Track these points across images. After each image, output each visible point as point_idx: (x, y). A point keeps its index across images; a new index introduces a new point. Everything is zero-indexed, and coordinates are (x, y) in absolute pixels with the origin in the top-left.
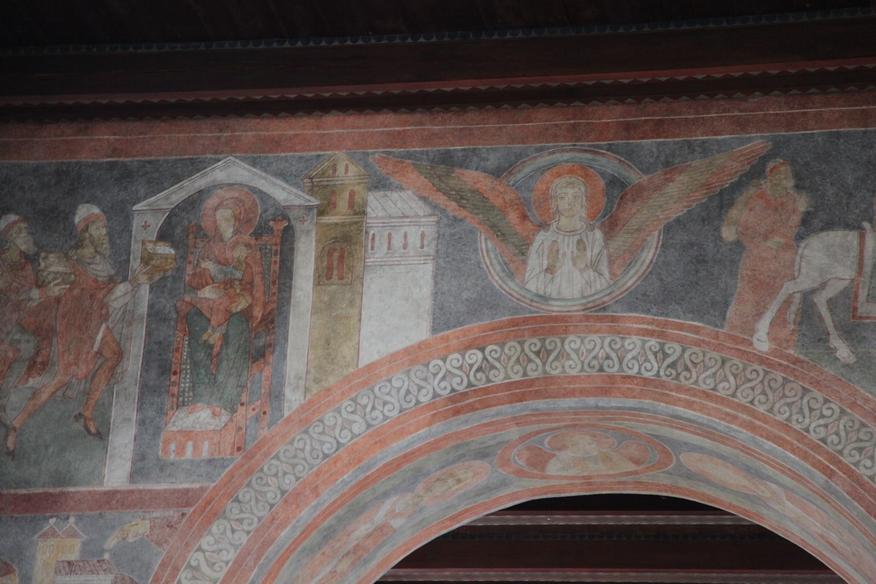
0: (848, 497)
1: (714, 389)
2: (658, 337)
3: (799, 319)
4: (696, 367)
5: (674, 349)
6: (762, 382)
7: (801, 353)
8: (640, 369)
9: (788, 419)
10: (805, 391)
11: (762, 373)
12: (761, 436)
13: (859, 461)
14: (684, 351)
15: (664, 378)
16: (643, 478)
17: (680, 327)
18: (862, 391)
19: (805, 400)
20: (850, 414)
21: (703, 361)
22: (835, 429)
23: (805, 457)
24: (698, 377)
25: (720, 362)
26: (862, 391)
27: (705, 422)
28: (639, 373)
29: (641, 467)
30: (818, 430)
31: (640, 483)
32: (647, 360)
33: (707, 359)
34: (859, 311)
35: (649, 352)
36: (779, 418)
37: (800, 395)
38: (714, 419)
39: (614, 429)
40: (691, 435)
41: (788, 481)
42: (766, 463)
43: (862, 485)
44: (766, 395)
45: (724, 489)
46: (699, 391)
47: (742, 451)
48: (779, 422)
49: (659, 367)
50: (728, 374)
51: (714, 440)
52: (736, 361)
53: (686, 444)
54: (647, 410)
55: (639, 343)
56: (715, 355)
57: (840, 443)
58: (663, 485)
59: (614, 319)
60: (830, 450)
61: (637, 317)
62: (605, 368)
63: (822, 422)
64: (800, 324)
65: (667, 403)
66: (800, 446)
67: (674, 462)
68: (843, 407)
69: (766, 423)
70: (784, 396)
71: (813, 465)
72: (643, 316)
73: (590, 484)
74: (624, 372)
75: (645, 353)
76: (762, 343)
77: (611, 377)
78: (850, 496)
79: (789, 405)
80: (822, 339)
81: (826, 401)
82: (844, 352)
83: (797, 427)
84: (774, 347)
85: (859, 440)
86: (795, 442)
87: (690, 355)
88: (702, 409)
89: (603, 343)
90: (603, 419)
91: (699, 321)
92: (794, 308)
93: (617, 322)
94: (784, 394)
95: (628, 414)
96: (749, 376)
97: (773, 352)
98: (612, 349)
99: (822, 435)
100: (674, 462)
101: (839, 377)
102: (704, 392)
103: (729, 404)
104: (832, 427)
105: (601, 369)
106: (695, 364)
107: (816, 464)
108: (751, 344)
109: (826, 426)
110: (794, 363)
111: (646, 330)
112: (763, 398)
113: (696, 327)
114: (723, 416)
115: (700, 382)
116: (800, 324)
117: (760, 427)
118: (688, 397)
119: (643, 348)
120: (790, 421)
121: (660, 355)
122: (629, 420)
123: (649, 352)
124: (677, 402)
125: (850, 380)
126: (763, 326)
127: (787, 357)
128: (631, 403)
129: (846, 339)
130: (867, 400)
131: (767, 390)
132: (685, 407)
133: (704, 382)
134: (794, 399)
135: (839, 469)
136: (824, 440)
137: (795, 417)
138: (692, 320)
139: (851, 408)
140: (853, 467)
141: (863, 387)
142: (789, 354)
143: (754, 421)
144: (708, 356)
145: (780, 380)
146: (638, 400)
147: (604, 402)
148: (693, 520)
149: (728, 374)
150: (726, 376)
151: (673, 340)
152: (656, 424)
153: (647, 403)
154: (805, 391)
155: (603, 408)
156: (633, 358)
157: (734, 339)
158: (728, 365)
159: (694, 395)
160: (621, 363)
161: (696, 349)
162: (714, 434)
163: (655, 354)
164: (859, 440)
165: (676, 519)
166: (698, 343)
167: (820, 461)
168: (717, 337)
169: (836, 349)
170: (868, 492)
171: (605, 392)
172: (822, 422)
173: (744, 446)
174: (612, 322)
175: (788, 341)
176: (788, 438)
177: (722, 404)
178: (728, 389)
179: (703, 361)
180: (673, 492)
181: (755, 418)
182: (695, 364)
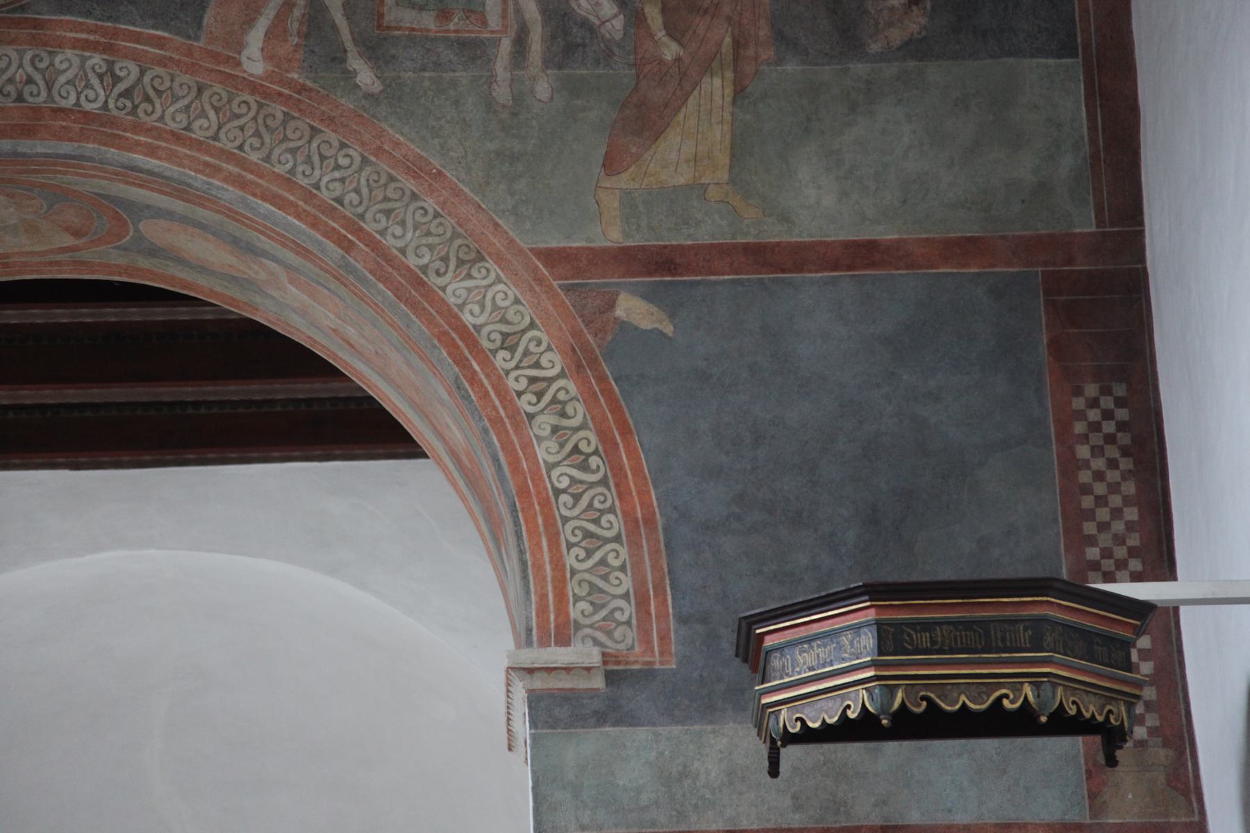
0: (370, 277)
1: (188, 128)
2: (104, 51)
3: (305, 29)
4: (160, 97)
5: (128, 70)
6: (255, 119)
7: (307, 77)
8: (78, 99)
9: (292, 171)
10: (315, 131)
11: (254, 106)
12: (254, 195)
13: (386, 229)
14: (142, 73)
15: (115, 112)
16: (85, 256)
17: (137, 38)
18: (391, 131)
19: (314, 145)
20: (375, 164)
21: (171, 88)
22: (354, 185)
23: (314, 225)
24: (164, 111)
25: (195, 89)
26: (391, 131)
27: (176, 176)
28: (78, 104)
29: (83, 240)
30: (331, 186)
31: (82, 263)
32: (88, 86)
33: (176, 85)
34: (386, 18)
35: (91, 75)
36: (279, 169)
37: (307, 137)
38: (188, 171)
39: (42, 185)
40: (155, 195)
41: (289, 256)
42: (261, 232)
43: (389, 259)
44: (260, 137)
45: (203, 269)
46: (166, 131)
47: (228, 216)
48: (279, 175)
49: (107, 97)
50: (207, 107)
51: (188, 201)
52: (218, 88)
53: (148, 207)
54: (91, 159)
55: (76, 62)
56: (186, 78)
57: (361, 203)
58: (118, 266)
59: (37, 24)
60: (348, 214)
61: (72, 22)
62: (26, 96)
63: (337, 174)
64: (307, 36)
65: (119, 148)
66: (308, 208)
67: (131, 234)
68: (366, 154)
69: (260, 177)
70: (286, 139)
71: (325, 235)
72: (80, 20)
73: (6, 265)
74: (54, 102)
75: (86, 75)
76: (254, 63)
77: (36, 111)
78: (374, 275)
79: (293, 151)
80: (337, 58)
81: (343, 145)
82: (366, 77)
83: (304, 182)
84: (270, 68)
85: (386, 199)
86: (301, 203)
87: (152, 80)
88: (171, 157)
89: (21, 59)
90: (26, 172)
91: (164, 30)
92: (297, 13)
93: (42, 28)
94: (285, 135)
95: (63, 165)
96: (237, 111)
97: (269, 76)
98: (35, 68)
99: (337, 193)
100: (131, 234)
101: (360, 112)
102: (173, 133)
103: (209, 151)
104: (351, 182)
105: (20, 98)
106: (159, 93)
107: (329, 233)
108: (239, 64)
109: (342, 180)
110: (299, 93)
111: (86, 41)
112: (256, 142)
113: (160, 38)
114: (201, 167)
115: (168, 119)
116: (307, 36)
117: (253, 183)
118: (150, 140)
119: (82, 67)
120: (294, 174)
121: (108, 79)
122: (65, 173)
123: (91, 75)
124: (133, 147)
125: (374, 116)
126: (255, 38)
127: (290, 84)
128: (66, 148)
129: (369, 59)
130: (397, 144)
131: (262, 129)
132: (146, 155)
133: (174, 119)
134: (299, 143)
135: (360, 240)
136: (339, 200)
137: (300, 169)
138: (153, 27)
139: (376, 156)
140: (377, 236)
141: (392, 126)
142: (292, 79)
143: (244, 173)
144: (178, 81)
145: (280, 116)
146: (76, 145)
147: (25, 146)
148: (159, 313)
149: (207, 107)
150: (203, 110)
151: (126, 57)
152: (105, 178)
153: (90, 147)
154: (315, 131)
155: (24, 155)
156: (68, 82)
157: (214, 56)
158: (206, 94)
159: (159, 138)
160: (49, 89)
161: (160, 71)
162: (188, 192)
163: (101, 77)
164: (386, 199)
165: (135, 314)
166: (162, 62)
167: (334, 229)
168: (189, 53)
169: (355, 72)
170: (398, 270)
171: (28, 131)
172: (337, 174)
173: (230, 210)
174: (35, 28)
175: (290, 61)
176: (291, 198)
177: (199, 150)
178: (207, 129)
179: (171, 88)
180: (129, 276)
181: (245, 170)
182: (159, 93)
